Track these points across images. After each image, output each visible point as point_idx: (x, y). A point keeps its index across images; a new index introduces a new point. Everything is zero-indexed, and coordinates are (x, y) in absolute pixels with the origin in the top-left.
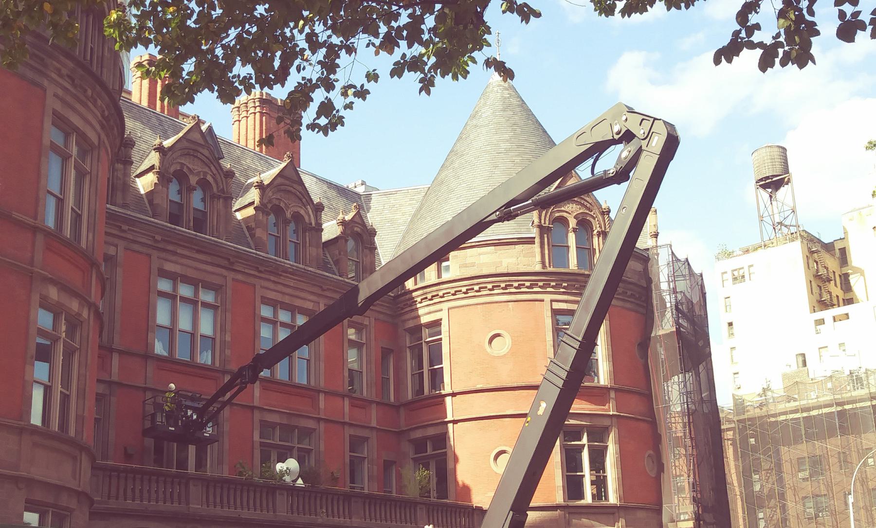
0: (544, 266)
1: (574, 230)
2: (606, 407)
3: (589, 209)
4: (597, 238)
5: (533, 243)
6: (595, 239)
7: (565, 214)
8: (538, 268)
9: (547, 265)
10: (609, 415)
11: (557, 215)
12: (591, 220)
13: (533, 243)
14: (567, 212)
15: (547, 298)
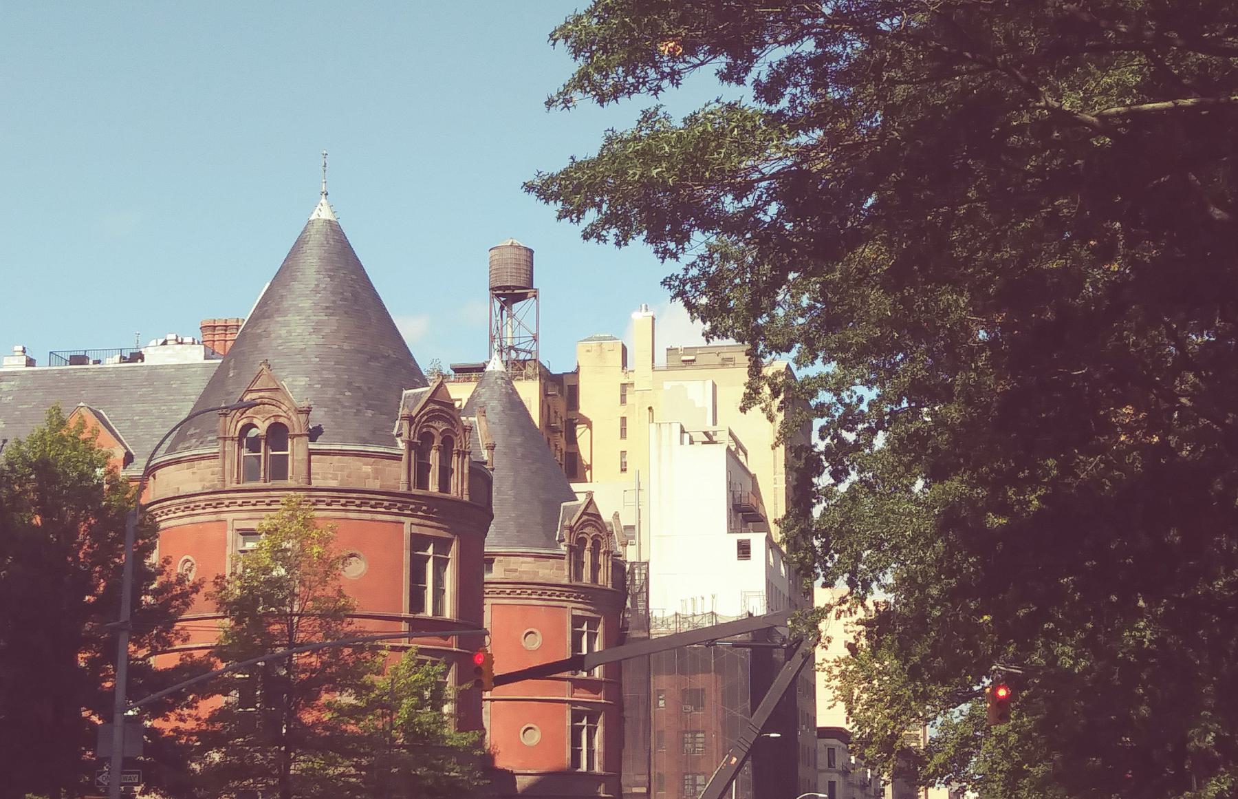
0: (409, 489)
1: (439, 449)
2: (449, 641)
3: (452, 425)
4: (456, 458)
5: (400, 459)
6: (455, 458)
7: (432, 430)
8: (403, 488)
9: (412, 485)
10: (452, 651)
11: (424, 430)
12: (455, 438)
13: (400, 459)
14: (432, 427)
15: (407, 521)
